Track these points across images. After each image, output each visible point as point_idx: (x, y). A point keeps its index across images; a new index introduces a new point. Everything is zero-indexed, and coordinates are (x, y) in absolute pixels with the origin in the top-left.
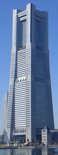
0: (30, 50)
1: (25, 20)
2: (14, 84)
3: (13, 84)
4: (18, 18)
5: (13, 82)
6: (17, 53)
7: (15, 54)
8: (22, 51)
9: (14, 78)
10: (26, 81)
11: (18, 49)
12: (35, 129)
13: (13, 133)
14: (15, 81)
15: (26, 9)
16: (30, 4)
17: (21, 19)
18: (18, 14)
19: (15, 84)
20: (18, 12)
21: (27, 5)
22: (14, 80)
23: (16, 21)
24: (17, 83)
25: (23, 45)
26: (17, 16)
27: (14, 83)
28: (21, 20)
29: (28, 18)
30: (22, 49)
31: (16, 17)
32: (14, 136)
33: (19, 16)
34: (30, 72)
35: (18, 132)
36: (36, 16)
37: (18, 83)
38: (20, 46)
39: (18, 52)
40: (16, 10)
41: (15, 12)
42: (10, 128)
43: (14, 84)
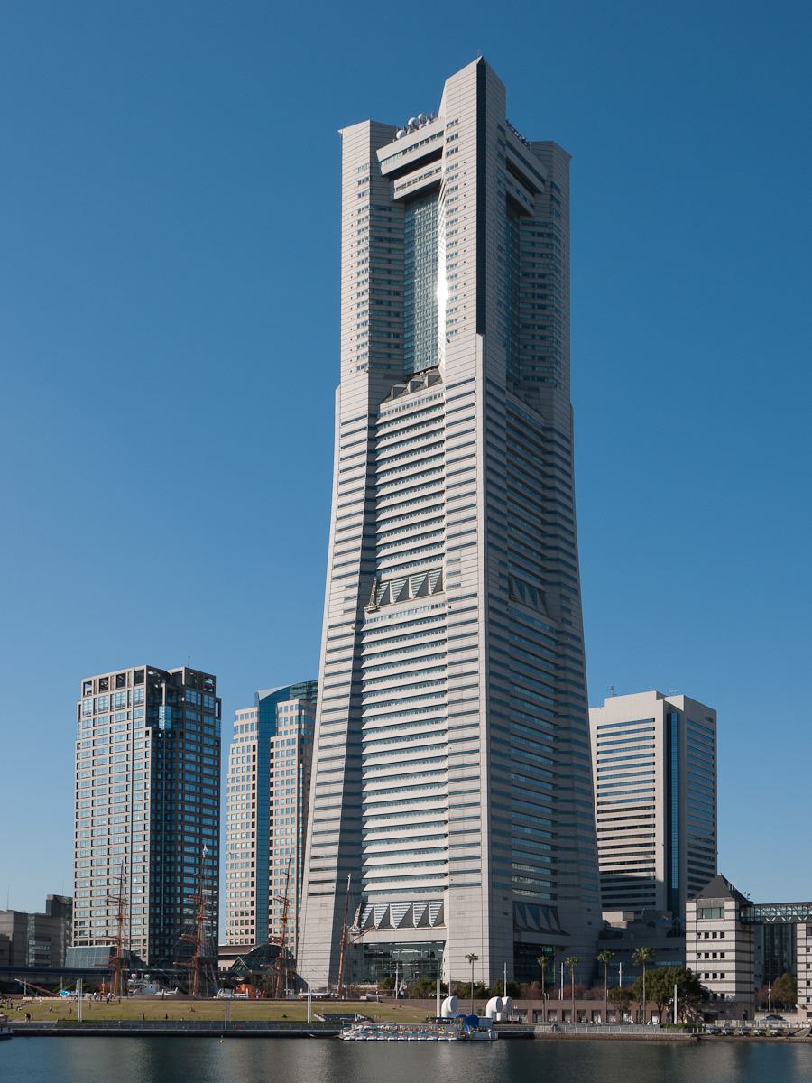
0: (478, 386)
1: (430, 193)
2: (360, 621)
3: (353, 616)
4: (380, 182)
5: (354, 604)
6: (373, 415)
7: (365, 423)
8: (409, 398)
9: (356, 579)
10: (448, 594)
11: (377, 396)
12: (510, 910)
13: (355, 929)
14: (363, 599)
15: (432, 113)
16: (471, 70)
17: (398, 183)
18: (382, 153)
19: (368, 616)
20: (381, 136)
21: (447, 81)
22: (355, 591)
23: (366, 201)
24: (377, 610)
25: (418, 367)
26: (375, 164)
27: (360, 610)
28: (397, 195)
29: (460, 172)
30: (416, 387)
31: (366, 173)
32: (356, 946)
33: (386, 169)
34: (480, 537)
35: (385, 924)
36: (511, 167)
37: (384, 610)
38: (395, 361)
39: (384, 407)
40: (368, 123)
41: (356, 138)
42: (332, 899)
43: (360, 621)
